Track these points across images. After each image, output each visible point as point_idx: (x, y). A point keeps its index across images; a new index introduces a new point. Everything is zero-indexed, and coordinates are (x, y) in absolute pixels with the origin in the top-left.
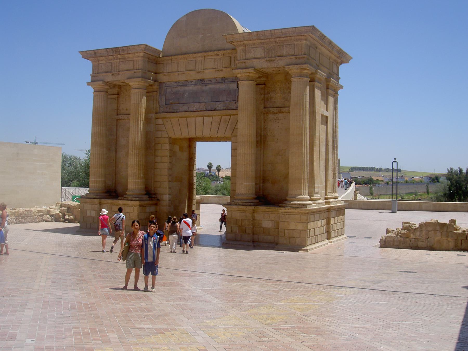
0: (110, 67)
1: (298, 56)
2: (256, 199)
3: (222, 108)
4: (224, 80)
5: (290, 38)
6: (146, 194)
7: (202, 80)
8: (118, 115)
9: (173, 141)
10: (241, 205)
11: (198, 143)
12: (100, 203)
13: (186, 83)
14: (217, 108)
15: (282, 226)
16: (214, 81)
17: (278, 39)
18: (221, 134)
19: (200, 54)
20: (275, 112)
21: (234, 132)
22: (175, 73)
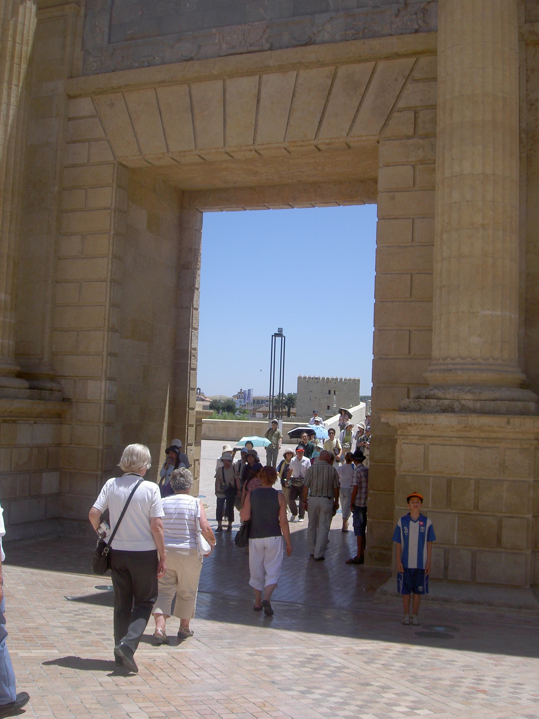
2: (523, 385)
6: (19, 375)
9: (132, 181)
10: (474, 411)
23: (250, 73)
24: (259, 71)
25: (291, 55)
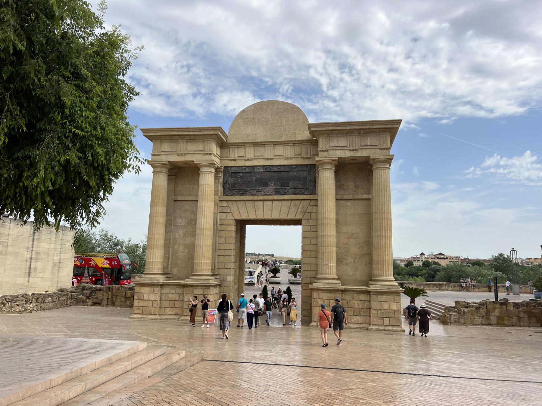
11: (247, 226)
18: (291, 216)
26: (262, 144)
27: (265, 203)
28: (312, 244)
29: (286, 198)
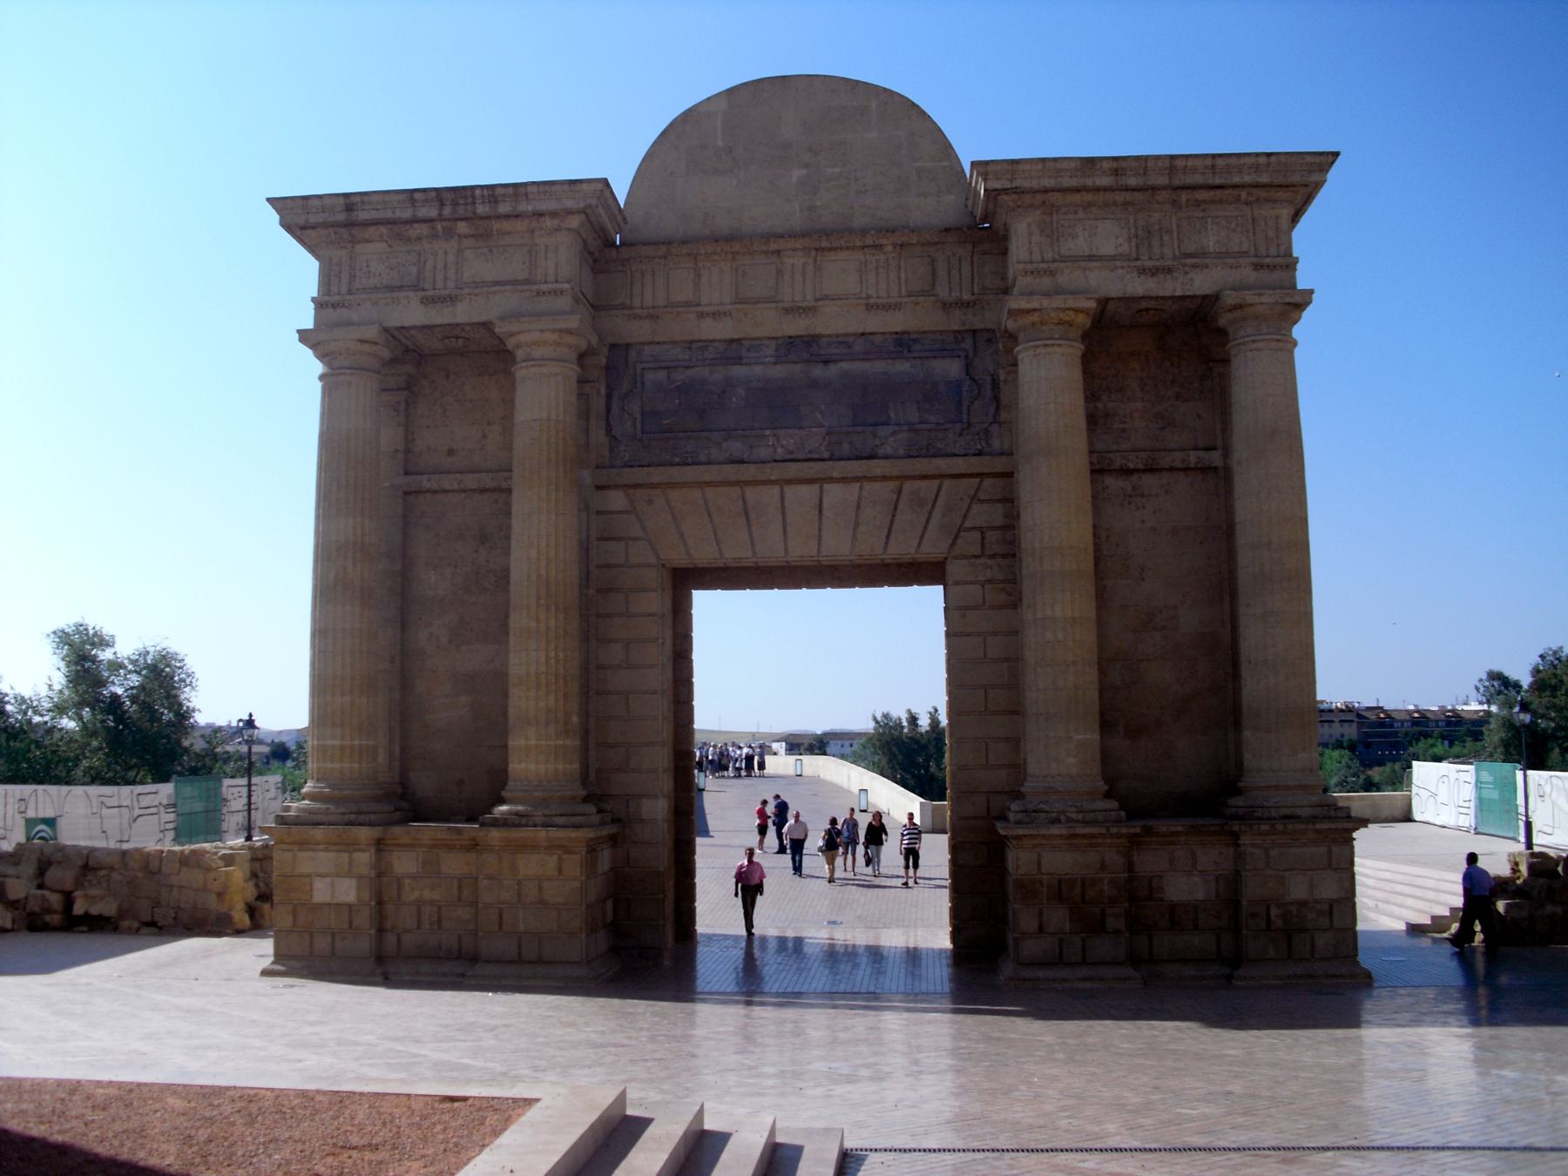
0: (414, 270)
1: (1267, 260)
3: (901, 452)
4: (903, 343)
5: (1235, 192)
7: (811, 340)
8: (406, 474)
12: (380, 845)
13: (734, 350)
14: (881, 451)
15: (1253, 889)
16: (859, 347)
17: (1184, 196)
19: (799, 244)
20: (1131, 466)
21: (960, 541)
22: (701, 309)
23: (810, 481)
24: (821, 481)
25: (855, 468)
26: (771, 242)
27: (792, 492)
28: (979, 659)
29: (878, 472)
